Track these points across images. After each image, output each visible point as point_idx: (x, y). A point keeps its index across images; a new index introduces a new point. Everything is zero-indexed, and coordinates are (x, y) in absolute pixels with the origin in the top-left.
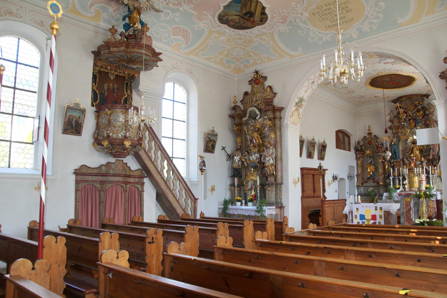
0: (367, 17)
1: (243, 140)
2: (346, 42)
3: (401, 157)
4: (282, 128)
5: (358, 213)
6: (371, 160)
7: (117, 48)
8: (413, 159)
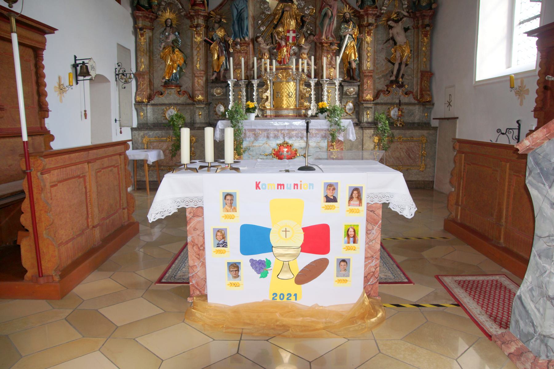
3: (251, 34)
5: (232, 217)
6: (175, 35)
8: (287, 39)
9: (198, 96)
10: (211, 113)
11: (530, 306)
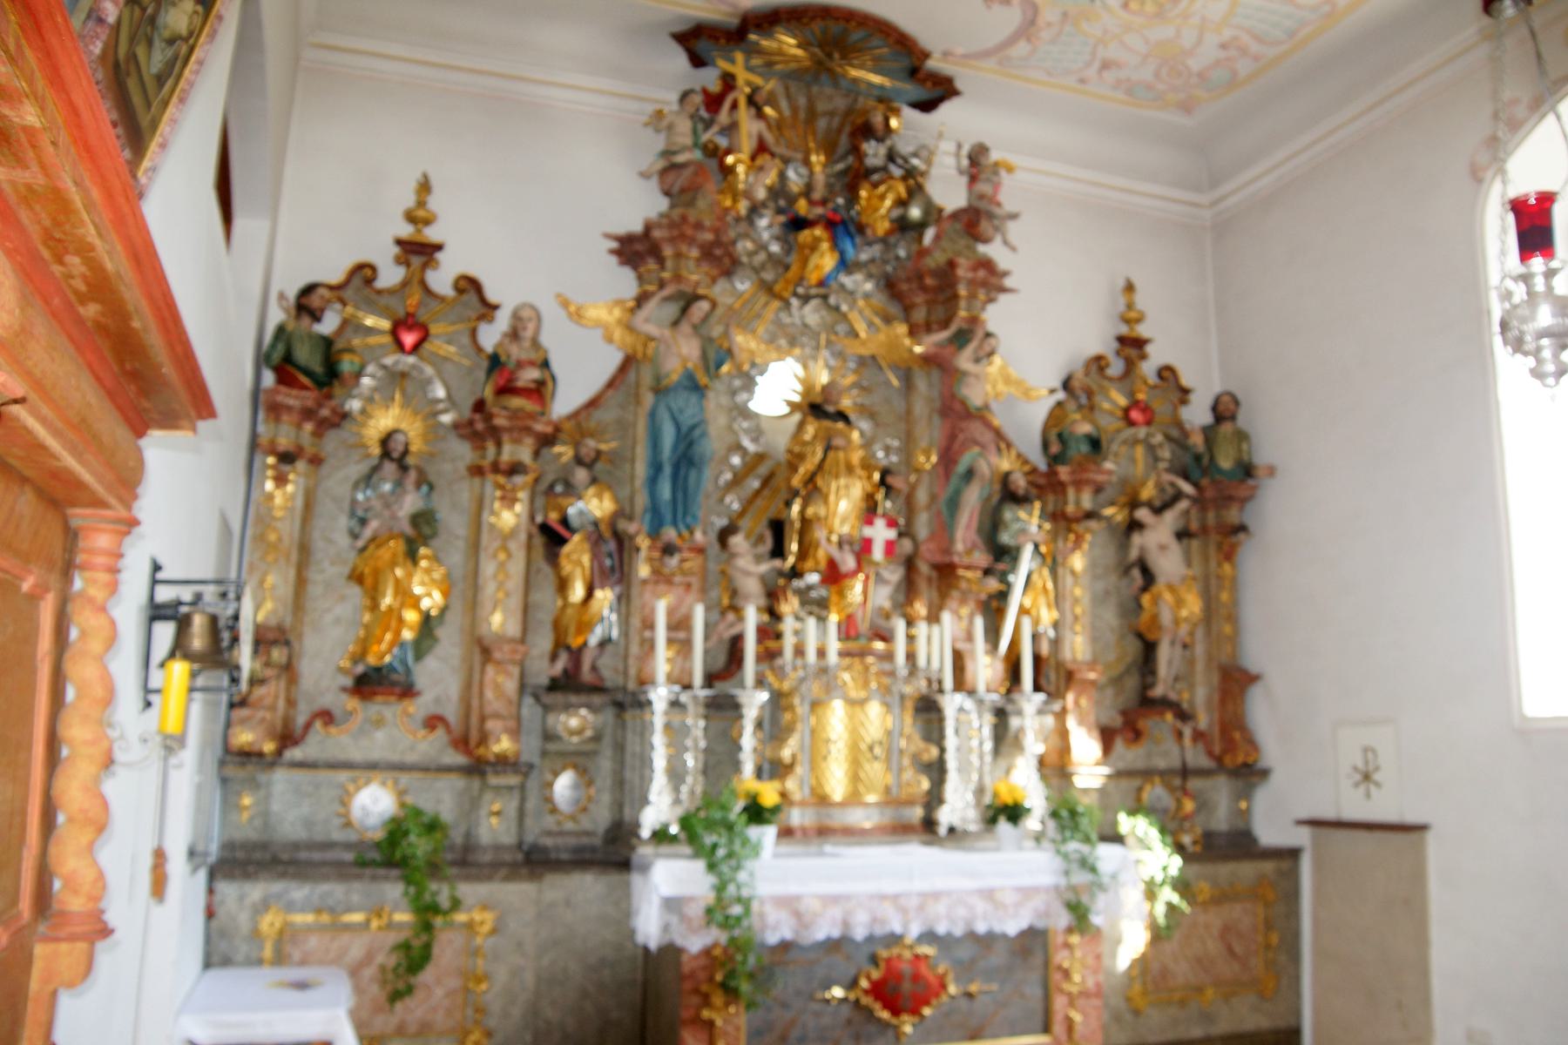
9: (498, 740)
10: (531, 805)
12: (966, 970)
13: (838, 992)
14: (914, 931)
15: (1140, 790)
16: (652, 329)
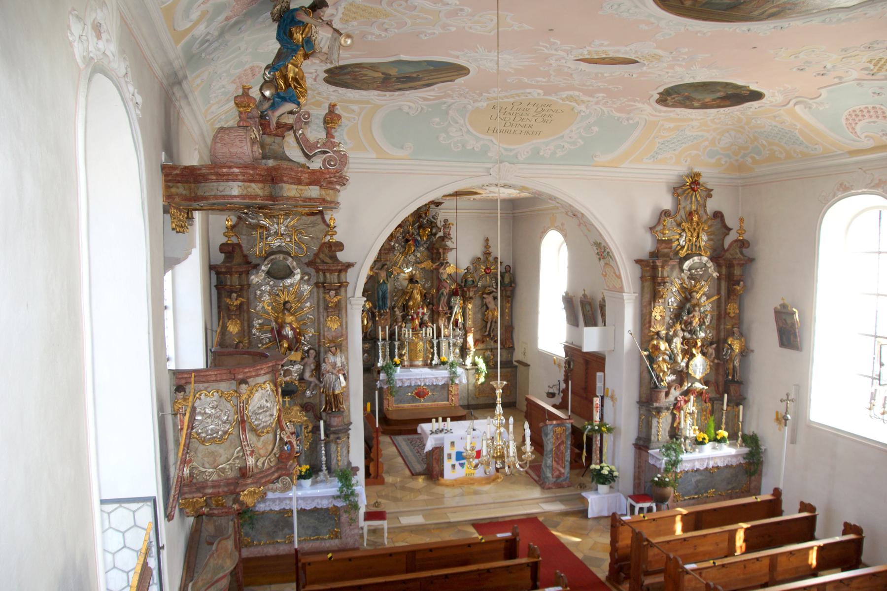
0: (563, 137)
1: (244, 327)
2: (505, 163)
4: (349, 307)
7: (296, 187)
11: (544, 469)
12: (433, 390)
13: (409, 394)
14: (423, 384)
15: (484, 353)
16: (377, 271)
